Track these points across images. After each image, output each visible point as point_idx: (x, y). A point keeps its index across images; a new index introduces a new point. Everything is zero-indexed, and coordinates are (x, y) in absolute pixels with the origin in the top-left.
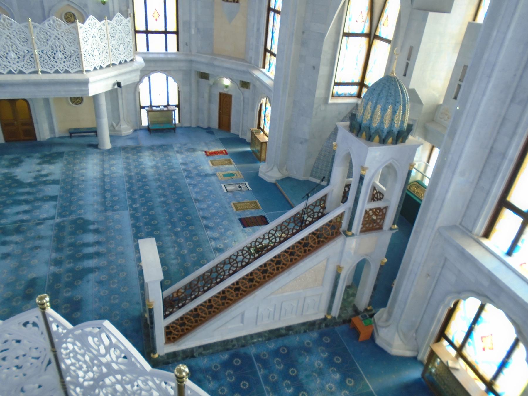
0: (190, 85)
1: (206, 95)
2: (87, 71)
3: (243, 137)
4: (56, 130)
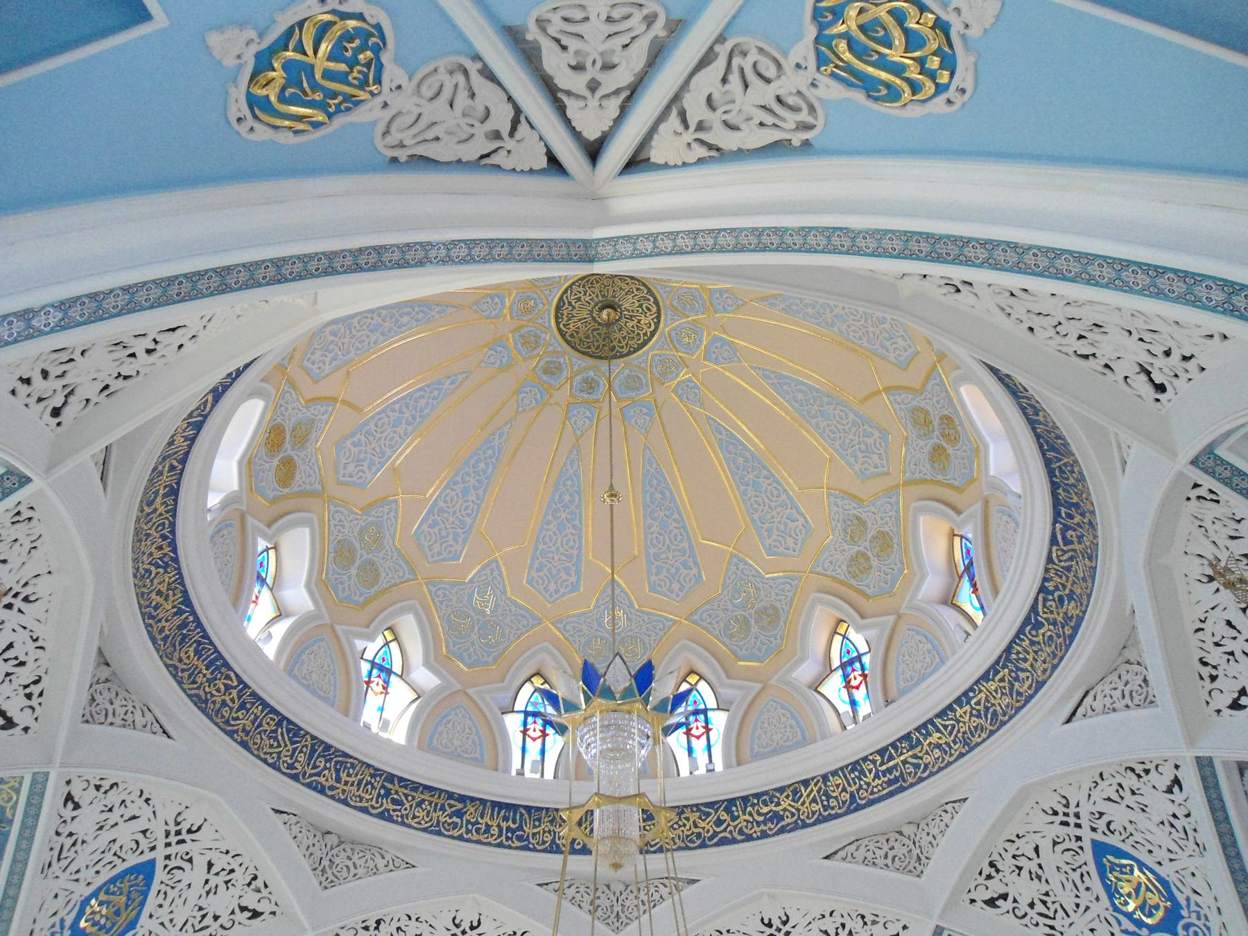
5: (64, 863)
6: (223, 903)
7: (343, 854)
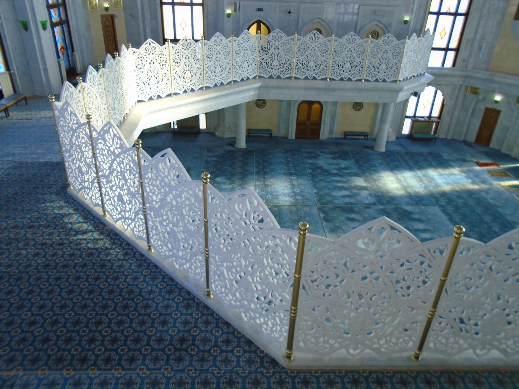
0: (457, 98)
1: (471, 110)
2: (400, 81)
3: (506, 152)
4: (335, 131)
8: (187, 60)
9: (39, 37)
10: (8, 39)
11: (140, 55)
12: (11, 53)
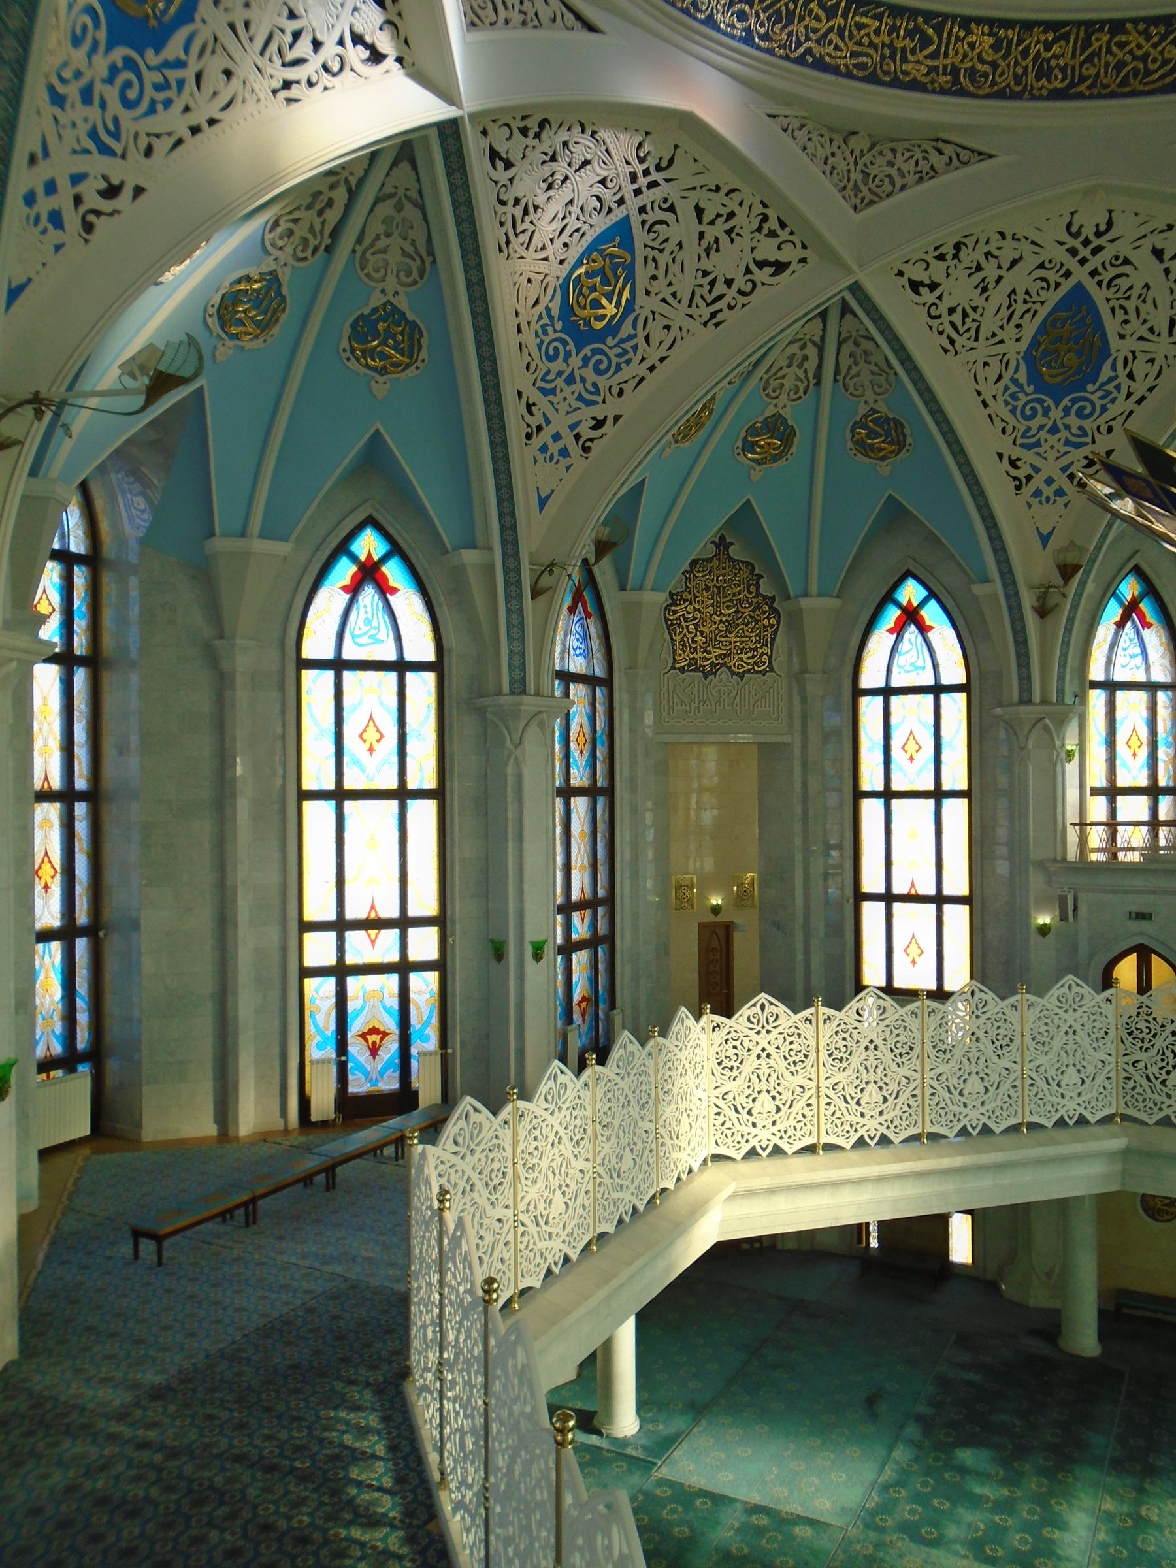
5: (524, 238)
6: (729, 261)
7: (880, 161)
8: (871, 1053)
9: (521, 978)
10: (458, 978)
11: (733, 1034)
12: (458, 1008)
